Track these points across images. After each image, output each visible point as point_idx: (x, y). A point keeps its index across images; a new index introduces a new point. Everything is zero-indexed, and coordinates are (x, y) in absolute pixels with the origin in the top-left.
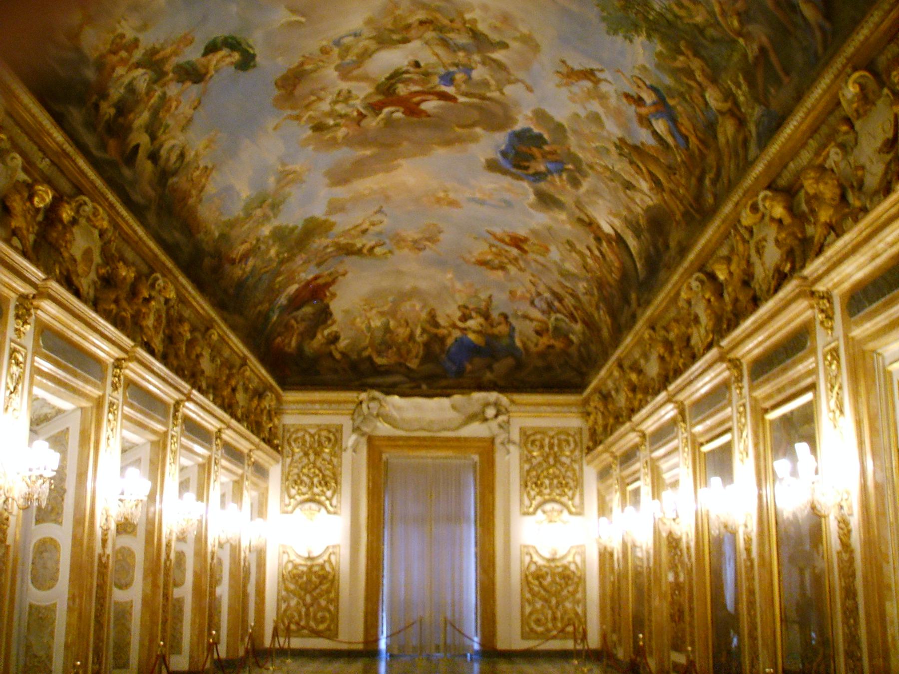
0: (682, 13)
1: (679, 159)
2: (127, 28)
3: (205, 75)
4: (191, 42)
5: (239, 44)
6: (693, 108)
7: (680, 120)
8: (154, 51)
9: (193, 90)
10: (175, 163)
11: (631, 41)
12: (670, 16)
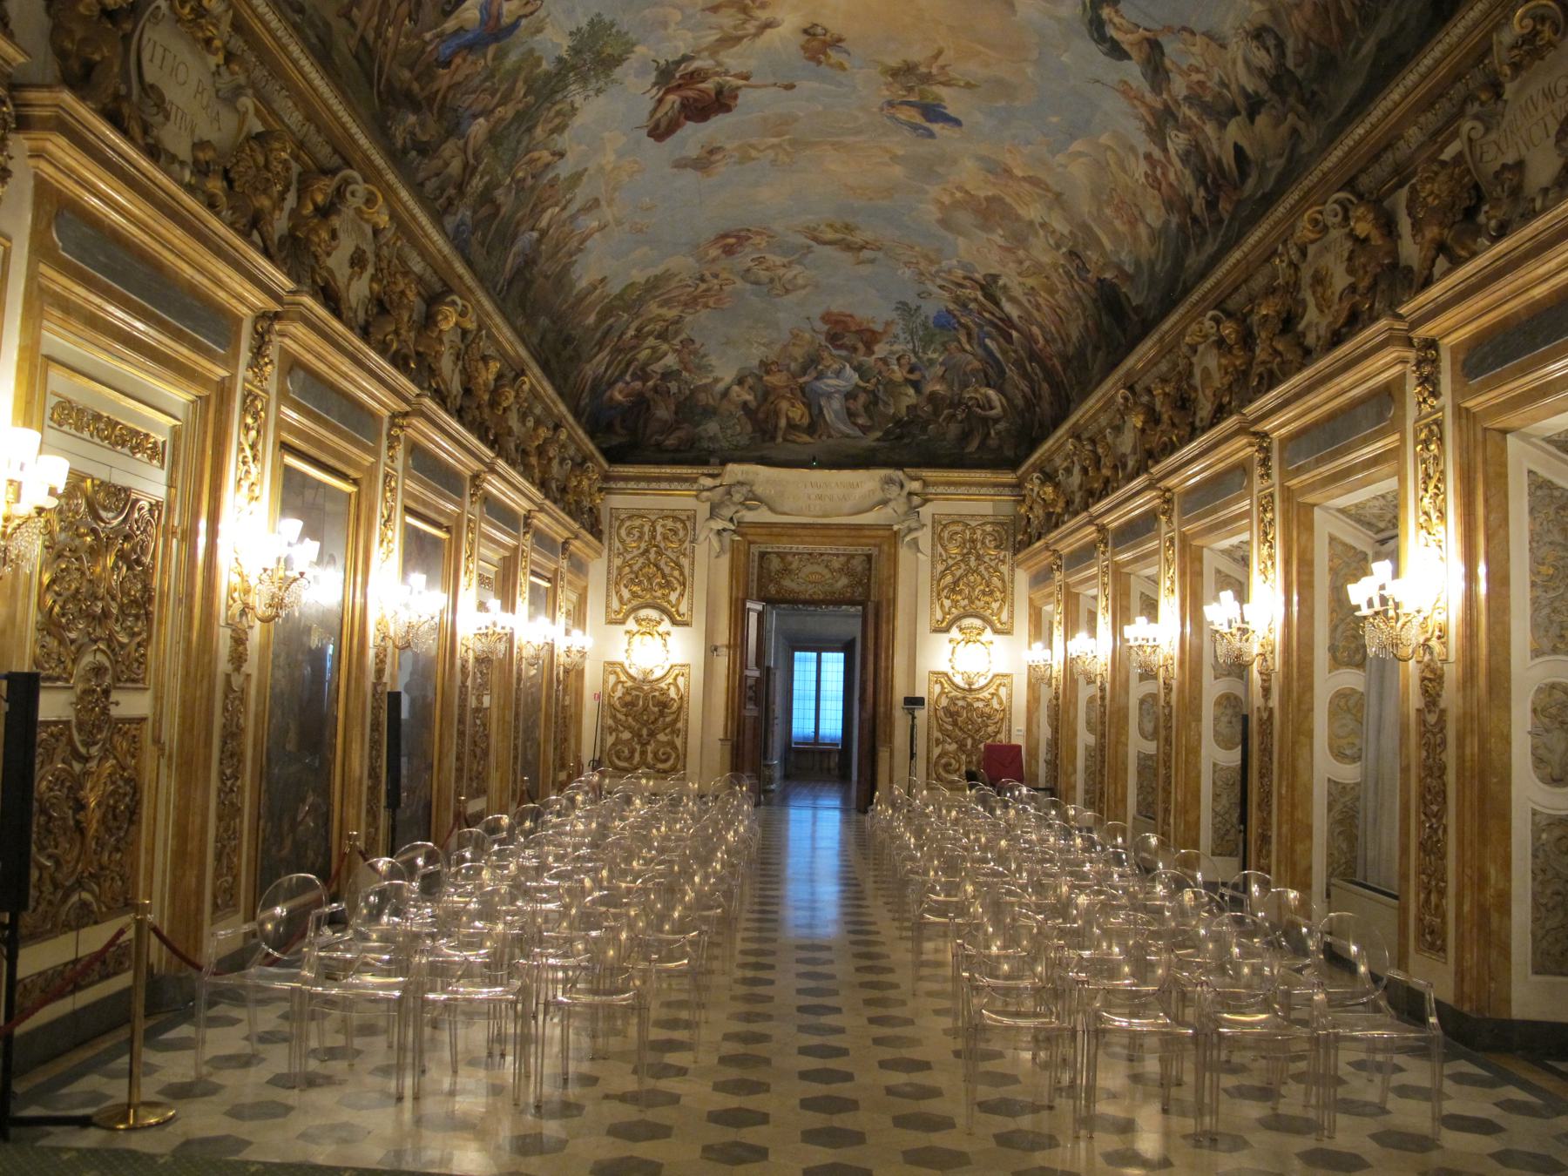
0: (552, 113)
1: (428, 36)
2: (1140, 169)
3: (1148, 40)
4: (1126, 82)
5: (1091, 22)
6: (474, 92)
7: (470, 58)
8: (1149, 131)
9: (1171, 47)
10: (1268, 51)
11: (571, 34)
12: (559, 97)
